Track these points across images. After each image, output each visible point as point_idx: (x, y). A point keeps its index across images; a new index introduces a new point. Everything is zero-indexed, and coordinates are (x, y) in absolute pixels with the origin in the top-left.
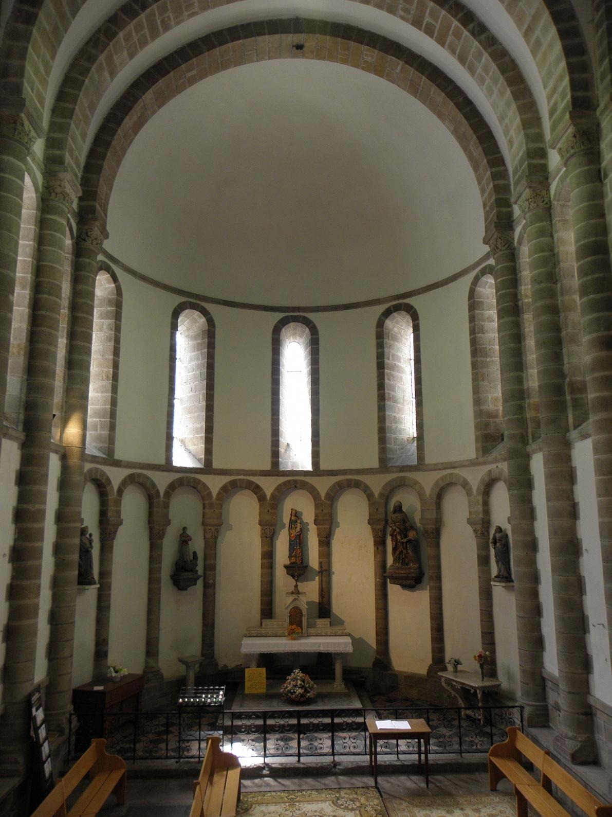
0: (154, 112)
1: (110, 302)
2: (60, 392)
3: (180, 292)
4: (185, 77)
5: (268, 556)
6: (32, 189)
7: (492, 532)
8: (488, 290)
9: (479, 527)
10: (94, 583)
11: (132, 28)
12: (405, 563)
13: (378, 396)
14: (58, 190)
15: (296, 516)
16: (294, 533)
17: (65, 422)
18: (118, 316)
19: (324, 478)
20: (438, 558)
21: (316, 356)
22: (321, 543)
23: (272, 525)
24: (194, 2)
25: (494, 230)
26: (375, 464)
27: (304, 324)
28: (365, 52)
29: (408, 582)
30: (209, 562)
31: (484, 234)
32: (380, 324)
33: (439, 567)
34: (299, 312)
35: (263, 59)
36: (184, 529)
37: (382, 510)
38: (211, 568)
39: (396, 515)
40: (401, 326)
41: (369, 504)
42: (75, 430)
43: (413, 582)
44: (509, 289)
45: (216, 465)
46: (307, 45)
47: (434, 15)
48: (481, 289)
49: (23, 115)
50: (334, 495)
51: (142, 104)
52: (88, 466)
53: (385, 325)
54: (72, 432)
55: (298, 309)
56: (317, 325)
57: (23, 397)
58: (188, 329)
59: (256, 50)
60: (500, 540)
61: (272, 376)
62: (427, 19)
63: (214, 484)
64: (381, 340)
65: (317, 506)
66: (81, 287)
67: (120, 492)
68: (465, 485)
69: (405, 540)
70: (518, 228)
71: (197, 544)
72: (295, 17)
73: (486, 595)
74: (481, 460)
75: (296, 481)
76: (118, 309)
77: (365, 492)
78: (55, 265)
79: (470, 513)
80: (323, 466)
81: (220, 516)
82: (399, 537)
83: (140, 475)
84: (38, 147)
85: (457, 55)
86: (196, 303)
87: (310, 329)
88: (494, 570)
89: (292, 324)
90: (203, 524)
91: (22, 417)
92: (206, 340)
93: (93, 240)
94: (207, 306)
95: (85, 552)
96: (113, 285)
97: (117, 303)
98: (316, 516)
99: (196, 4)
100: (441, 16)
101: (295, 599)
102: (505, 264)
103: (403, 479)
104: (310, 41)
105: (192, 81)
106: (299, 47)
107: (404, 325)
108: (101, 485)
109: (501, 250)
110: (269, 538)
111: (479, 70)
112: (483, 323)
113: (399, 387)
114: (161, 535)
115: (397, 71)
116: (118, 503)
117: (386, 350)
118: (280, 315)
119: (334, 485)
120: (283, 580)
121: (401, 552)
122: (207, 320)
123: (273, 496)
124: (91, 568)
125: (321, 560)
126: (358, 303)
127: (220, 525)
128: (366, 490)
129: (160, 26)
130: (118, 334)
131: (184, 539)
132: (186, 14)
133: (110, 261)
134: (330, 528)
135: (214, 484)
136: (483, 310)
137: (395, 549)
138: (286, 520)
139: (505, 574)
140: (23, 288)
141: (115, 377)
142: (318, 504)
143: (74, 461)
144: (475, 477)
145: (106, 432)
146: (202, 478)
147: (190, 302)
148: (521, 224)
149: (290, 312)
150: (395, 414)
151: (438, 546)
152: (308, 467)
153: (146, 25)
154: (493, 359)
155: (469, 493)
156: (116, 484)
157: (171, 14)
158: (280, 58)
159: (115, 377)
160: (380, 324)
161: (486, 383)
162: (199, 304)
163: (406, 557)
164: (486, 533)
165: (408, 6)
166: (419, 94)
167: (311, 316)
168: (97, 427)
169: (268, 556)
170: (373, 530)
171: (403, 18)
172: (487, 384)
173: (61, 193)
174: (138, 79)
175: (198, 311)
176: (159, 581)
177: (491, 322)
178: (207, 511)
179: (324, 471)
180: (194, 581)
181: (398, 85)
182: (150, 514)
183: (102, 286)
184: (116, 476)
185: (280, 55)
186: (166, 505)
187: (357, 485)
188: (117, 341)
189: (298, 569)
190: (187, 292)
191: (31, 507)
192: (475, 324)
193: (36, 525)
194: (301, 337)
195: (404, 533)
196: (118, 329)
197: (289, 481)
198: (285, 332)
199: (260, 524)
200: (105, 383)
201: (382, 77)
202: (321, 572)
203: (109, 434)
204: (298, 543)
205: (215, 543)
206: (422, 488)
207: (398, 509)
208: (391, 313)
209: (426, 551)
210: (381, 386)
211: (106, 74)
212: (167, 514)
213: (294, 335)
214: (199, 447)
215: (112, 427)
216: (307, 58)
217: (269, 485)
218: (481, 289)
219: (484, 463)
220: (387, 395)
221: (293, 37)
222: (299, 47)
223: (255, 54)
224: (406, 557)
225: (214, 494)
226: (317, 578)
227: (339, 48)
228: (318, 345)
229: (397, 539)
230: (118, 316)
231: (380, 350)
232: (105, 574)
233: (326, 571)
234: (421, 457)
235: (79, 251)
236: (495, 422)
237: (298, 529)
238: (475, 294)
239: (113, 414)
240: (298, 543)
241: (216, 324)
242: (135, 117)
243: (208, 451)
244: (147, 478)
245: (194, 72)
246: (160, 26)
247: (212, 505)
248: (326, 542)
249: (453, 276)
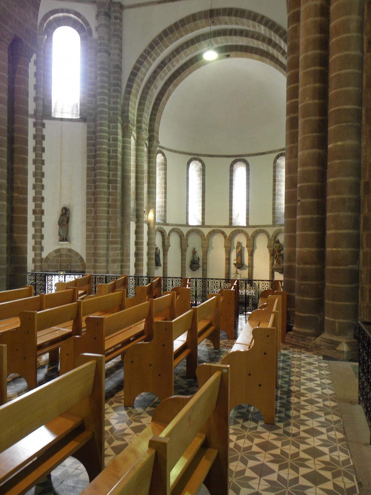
1: (162, 164)
5: (228, 260)
6: (133, 140)
10: (161, 266)
12: (279, 263)
14: (141, 138)
15: (239, 244)
16: (238, 251)
17: (148, 212)
18: (165, 169)
19: (250, 229)
22: (249, 255)
23: (229, 248)
26: (271, 223)
30: (204, 261)
32: (275, 162)
36: (194, 248)
38: (205, 263)
45: (206, 224)
50: (254, 236)
52: (156, 227)
57: (135, 208)
63: (206, 231)
65: (247, 240)
66: (151, 165)
67: (169, 235)
71: (200, 254)
75: (239, 230)
77: (266, 234)
80: (250, 224)
81: (208, 244)
83: (176, 228)
84: (134, 134)
89: (239, 163)
90: (202, 247)
91: (135, 214)
92: (202, 173)
94: (202, 158)
95: (157, 255)
96: (163, 157)
97: (165, 164)
98: (247, 244)
101: (235, 276)
108: (162, 233)
110: (228, 252)
114: (185, 251)
116: (168, 238)
118: (233, 159)
119: (254, 232)
120: (233, 269)
123: (230, 236)
124: (160, 260)
127: (208, 247)
128: (267, 234)
131: (194, 252)
135: (206, 231)
138: (235, 246)
140: (133, 173)
141: (165, 193)
142: (248, 240)
143: (152, 225)
145: (163, 214)
146: (201, 229)
150: (281, 202)
152: (245, 225)
156: (167, 232)
159: (165, 193)
160: (275, 162)
163: (280, 261)
167: (246, 158)
169: (228, 260)
170: (269, 250)
174: (166, 81)
176: (185, 267)
178: (203, 242)
180: (198, 268)
182: (181, 243)
183: (159, 158)
184: (167, 229)
186: (187, 240)
187: (264, 231)
188: (166, 179)
189: (240, 265)
191: (139, 241)
193: (141, 246)
196: (166, 174)
197: (236, 230)
199: (225, 247)
200: (162, 195)
202: (249, 266)
204: (240, 254)
205: (207, 254)
210: (274, 190)
212: (187, 243)
214: (200, 217)
215: (165, 211)
217: (228, 232)
225: (206, 236)
226: (248, 269)
230: (165, 169)
231: (274, 174)
232: (165, 263)
233: (251, 266)
235: (150, 152)
237: (240, 249)
239: (165, 207)
240: (240, 254)
243: (203, 218)
244: (179, 229)
247: (205, 240)
248: (251, 255)
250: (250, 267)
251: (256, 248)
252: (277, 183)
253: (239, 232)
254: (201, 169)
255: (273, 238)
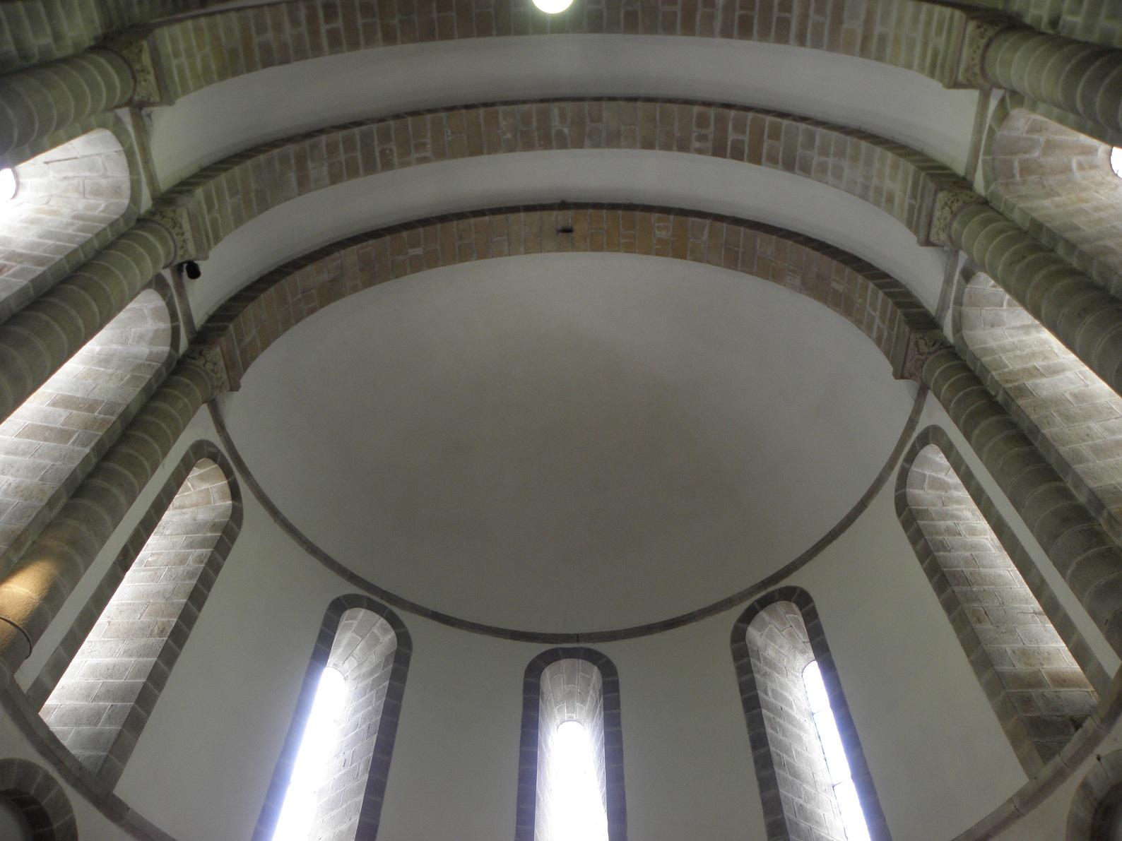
0: (355, 289)
2: (30, 516)
3: (352, 578)
4: (407, 253)
8: (930, 491)
11: (340, 139)
13: (756, 761)
21: (614, 711)
24: (427, 143)
25: (907, 329)
27: (587, 660)
28: (657, 224)
31: (892, 369)
32: (739, 636)
34: (578, 641)
35: (517, 253)
40: (781, 647)
42: (24, 589)
44: (969, 387)
46: (576, 228)
47: (739, 128)
48: (917, 491)
49: (145, 44)
51: (339, 261)
53: (747, 633)
54: (14, 590)
55: (577, 638)
56: (614, 661)
58: (360, 665)
59: (508, 235)
61: (521, 746)
62: (732, 136)
70: (946, 319)
72: (559, 201)
74: (1046, 771)
76: (224, 537)
78: (114, 269)
85: (780, 163)
86: (381, 605)
87: (599, 668)
89: (565, 663)
93: (206, 362)
94: (403, 615)
96: (229, 502)
99: (429, 146)
100: (749, 122)
102: (945, 366)
104: (582, 223)
105: (417, 265)
106: (568, 231)
107: (787, 647)
109: (929, 353)
111: (816, 159)
112: (941, 538)
113: (798, 753)
115: (705, 238)
122: (398, 636)
126: (691, 614)
129: (378, 159)
130: (211, 572)
132: (415, 156)
133: (237, 467)
136: (932, 520)
147: (369, 600)
148: (949, 308)
149: (562, 643)
150: (801, 802)
153: (359, 146)
157: (394, 147)
158: (541, 252)
160: (739, 636)
161: (988, 626)
162: (386, 608)
165: (704, 132)
166: (740, 261)
168: (99, 719)
171: (700, 151)
172: (991, 627)
173: (172, 219)
175: (382, 616)
181: (708, 262)
185: (541, 245)
190: (368, 583)
192: (925, 539)
194: (583, 702)
198: (552, 680)
201: (684, 257)
203: (121, 731)
208: (757, 612)
211: (292, 177)
213: (569, 696)
216: (578, 250)
218: (917, 491)
219: (1061, 775)
220: (775, 759)
221: (557, 216)
222: (568, 231)
223: (506, 243)
227: (621, 226)
228: (618, 691)
236: (1043, 695)
238: (908, 499)
241: (413, 641)
242: (325, 277)
245: (418, 251)
246: (378, 159)
249: (859, 503)
254: (387, 658)
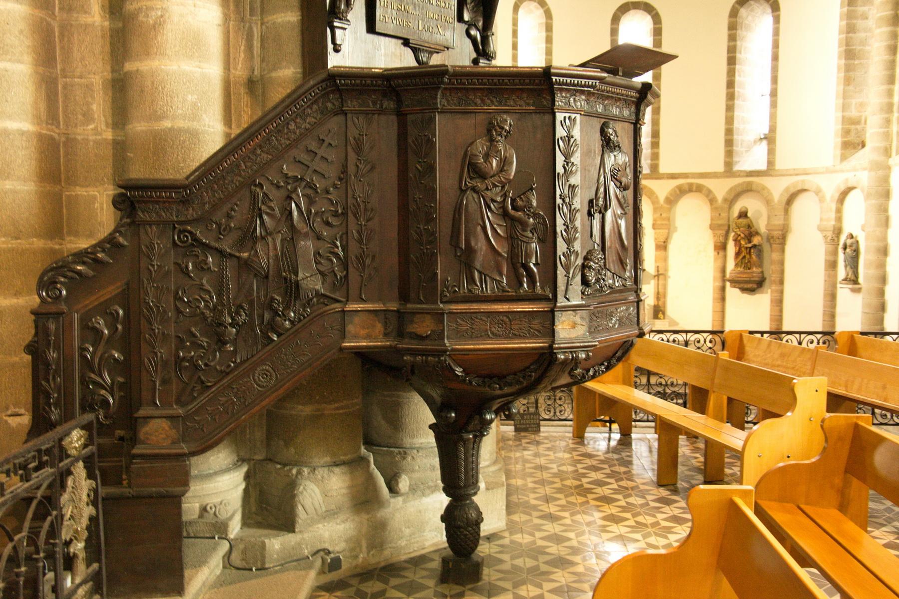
7: (843, 238)
9: (830, 234)
20: (782, 263)
26: (720, 168)
29: (750, 286)
32: (734, 13)
33: (782, 272)
37: (724, 215)
39: (741, 220)
41: (712, 209)
43: (755, 286)
53: (740, 14)
60: (851, 246)
64: (734, 32)
68: (818, 192)
69: (750, 245)
73: (831, 297)
77: (707, 196)
79: (821, 220)
82: (743, 242)
88: (842, 272)
98: (655, 220)
103: (750, 183)
117: (738, 43)
119: (674, 190)
121: (744, 257)
125: (658, 264)
134: (668, 233)
137: (738, 254)
139: (853, 278)
144: (830, 186)
151: (783, 251)
154: (862, 61)
155: (822, 200)
163: (749, 262)
164: (836, 239)
177: (864, 19)
179: (664, 174)
187: (699, 189)
195: (749, 237)
202: (658, 276)
206: (770, 194)
207: (743, 215)
209: (771, 256)
210: (731, 84)
219: (842, 171)
220: (736, 94)
224: (749, 262)
229: (741, 244)
231: (732, 44)
234: (771, 163)
250: (661, 277)
251: (675, 229)
252: (737, 67)
253: (690, 190)
255: (726, 206)
